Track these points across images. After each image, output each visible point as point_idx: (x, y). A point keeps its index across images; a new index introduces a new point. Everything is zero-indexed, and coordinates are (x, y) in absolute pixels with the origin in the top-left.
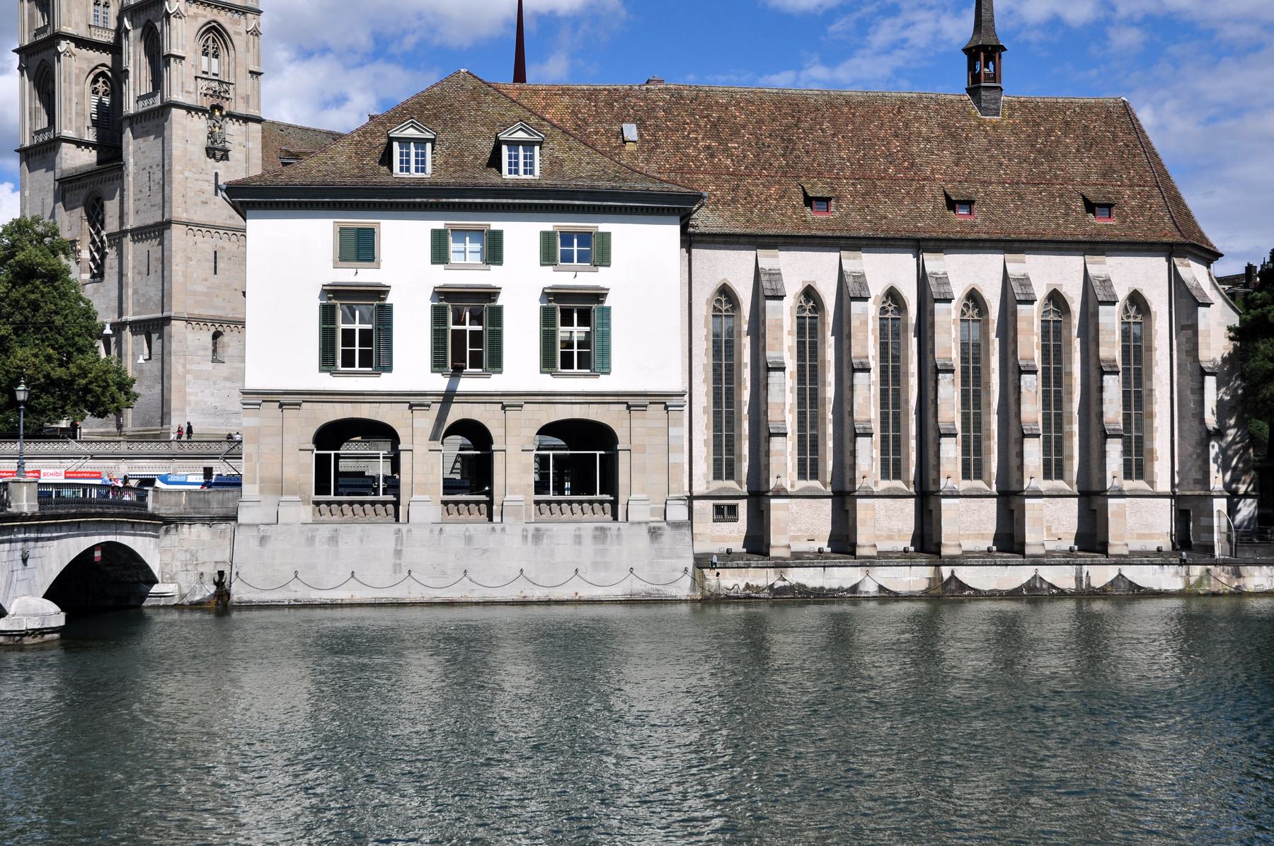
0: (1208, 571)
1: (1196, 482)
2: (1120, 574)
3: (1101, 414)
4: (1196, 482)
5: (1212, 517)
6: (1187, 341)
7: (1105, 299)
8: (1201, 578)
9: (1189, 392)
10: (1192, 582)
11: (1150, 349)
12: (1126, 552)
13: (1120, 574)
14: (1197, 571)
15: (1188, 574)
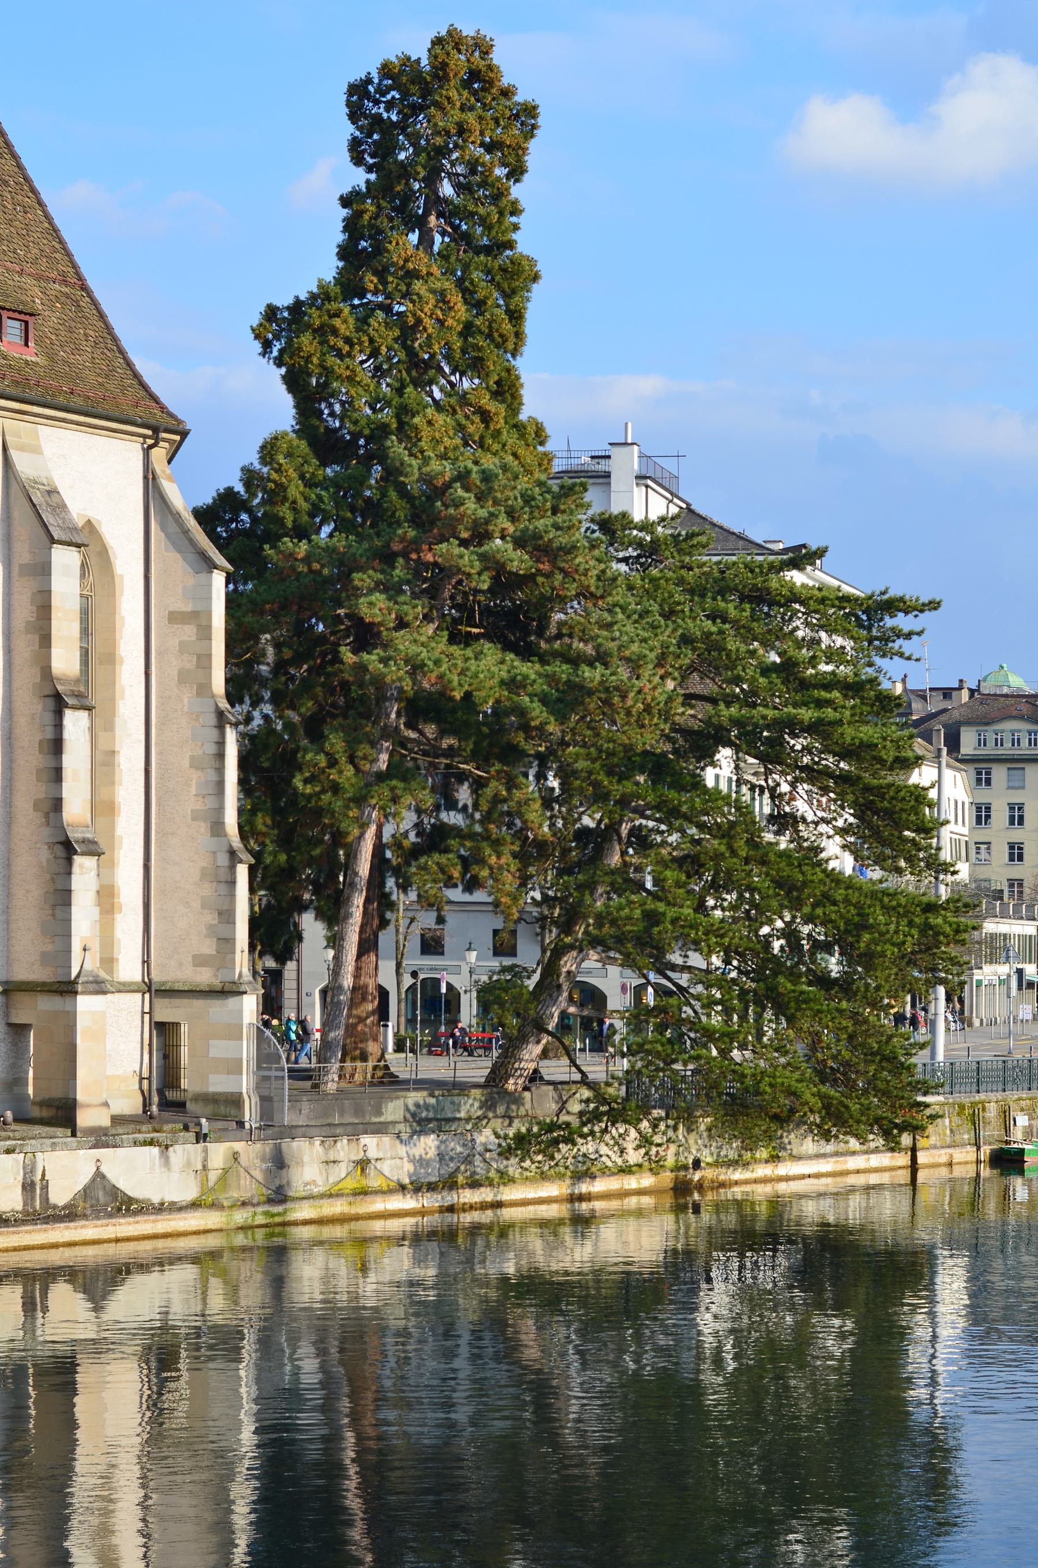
0: (235, 1156)
1: (200, 961)
2: (99, 1175)
3: (57, 804)
4: (200, 961)
5: (241, 1039)
6: (183, 647)
7: (64, 538)
8: (226, 1171)
9: (186, 763)
10: (211, 1184)
11: (111, 659)
12: (106, 1122)
13: (99, 1175)
14: (218, 1153)
15: (205, 1168)
